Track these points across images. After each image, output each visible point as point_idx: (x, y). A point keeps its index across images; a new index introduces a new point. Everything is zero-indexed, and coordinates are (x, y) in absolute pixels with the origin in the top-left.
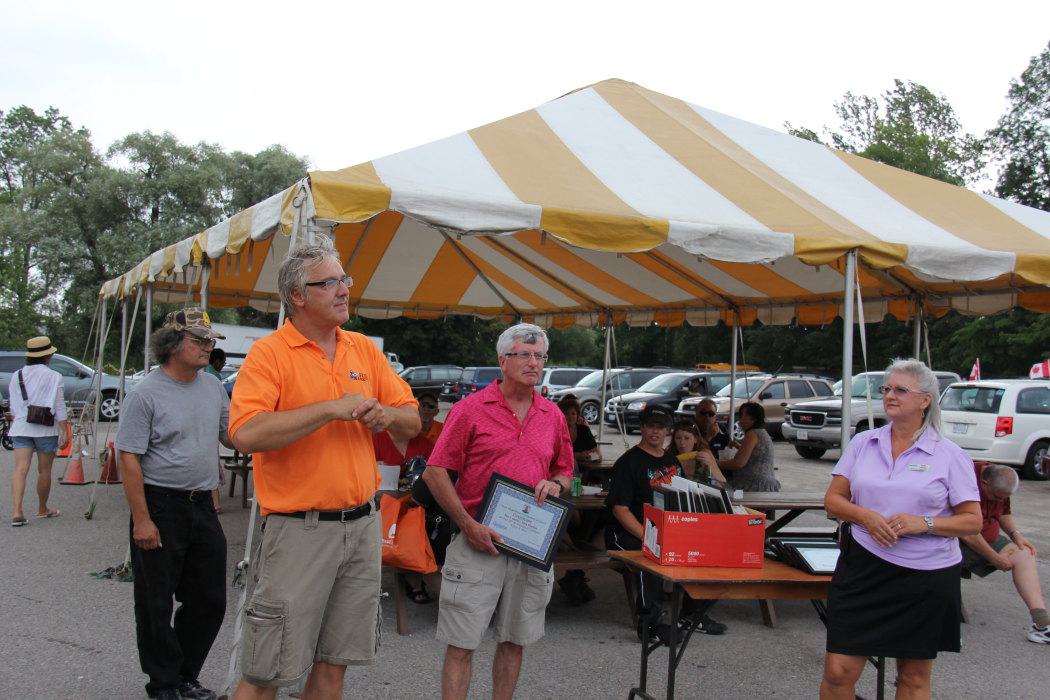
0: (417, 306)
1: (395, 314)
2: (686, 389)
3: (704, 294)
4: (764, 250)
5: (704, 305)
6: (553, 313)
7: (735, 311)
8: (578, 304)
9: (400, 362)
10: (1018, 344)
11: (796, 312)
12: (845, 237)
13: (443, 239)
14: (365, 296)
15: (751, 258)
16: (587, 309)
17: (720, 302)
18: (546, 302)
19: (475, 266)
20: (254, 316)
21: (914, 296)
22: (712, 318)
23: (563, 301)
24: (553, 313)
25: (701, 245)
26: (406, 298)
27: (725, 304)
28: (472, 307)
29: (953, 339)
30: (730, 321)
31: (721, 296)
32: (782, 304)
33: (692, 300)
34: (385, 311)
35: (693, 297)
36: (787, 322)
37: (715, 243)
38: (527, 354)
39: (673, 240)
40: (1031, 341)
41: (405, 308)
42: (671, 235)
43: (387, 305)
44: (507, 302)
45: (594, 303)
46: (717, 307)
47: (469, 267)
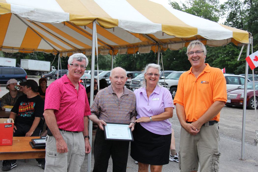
0: (24, 49)
1: (17, 51)
3: (103, 45)
6: (67, 52)
8: (72, 49)
9: (56, 69)
10: (231, 64)
11: (127, 50)
13: (27, 27)
14: (3, 45)
16: (75, 50)
17: (107, 47)
18: (66, 49)
19: (41, 37)
20: (10, 55)
21: (157, 44)
23: (69, 48)
24: (67, 52)
26: (19, 47)
28: (43, 50)
29: (213, 63)
32: (124, 48)
34: (12, 50)
36: (125, 53)
40: (235, 64)
41: (19, 49)
43: (13, 48)
44: (54, 48)
45: (76, 48)
47: (40, 37)
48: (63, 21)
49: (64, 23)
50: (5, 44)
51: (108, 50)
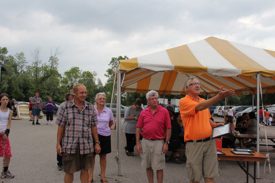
2: (255, 111)
4: (234, 73)
5: (246, 90)
7: (253, 91)
12: (257, 69)
14: (172, 90)
15: (230, 75)
17: (249, 89)
22: (248, 93)
25: (216, 73)
27: (251, 89)
30: (252, 93)
31: (249, 87)
33: (243, 88)
35: (243, 88)
37: (220, 72)
38: (153, 99)
39: (209, 72)
42: (208, 70)
46: (249, 90)
48: (237, 75)
49: (238, 76)
50: (173, 89)
51: (249, 91)
